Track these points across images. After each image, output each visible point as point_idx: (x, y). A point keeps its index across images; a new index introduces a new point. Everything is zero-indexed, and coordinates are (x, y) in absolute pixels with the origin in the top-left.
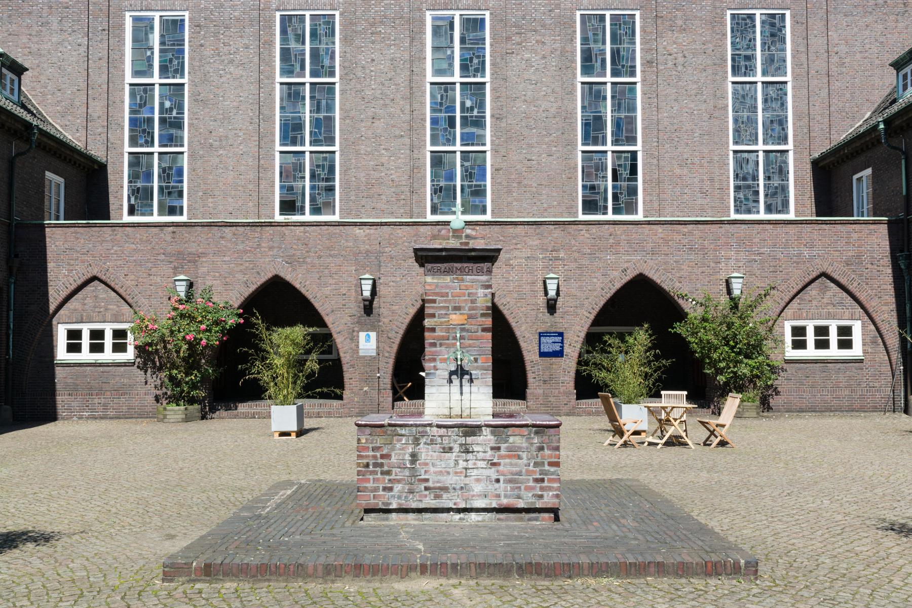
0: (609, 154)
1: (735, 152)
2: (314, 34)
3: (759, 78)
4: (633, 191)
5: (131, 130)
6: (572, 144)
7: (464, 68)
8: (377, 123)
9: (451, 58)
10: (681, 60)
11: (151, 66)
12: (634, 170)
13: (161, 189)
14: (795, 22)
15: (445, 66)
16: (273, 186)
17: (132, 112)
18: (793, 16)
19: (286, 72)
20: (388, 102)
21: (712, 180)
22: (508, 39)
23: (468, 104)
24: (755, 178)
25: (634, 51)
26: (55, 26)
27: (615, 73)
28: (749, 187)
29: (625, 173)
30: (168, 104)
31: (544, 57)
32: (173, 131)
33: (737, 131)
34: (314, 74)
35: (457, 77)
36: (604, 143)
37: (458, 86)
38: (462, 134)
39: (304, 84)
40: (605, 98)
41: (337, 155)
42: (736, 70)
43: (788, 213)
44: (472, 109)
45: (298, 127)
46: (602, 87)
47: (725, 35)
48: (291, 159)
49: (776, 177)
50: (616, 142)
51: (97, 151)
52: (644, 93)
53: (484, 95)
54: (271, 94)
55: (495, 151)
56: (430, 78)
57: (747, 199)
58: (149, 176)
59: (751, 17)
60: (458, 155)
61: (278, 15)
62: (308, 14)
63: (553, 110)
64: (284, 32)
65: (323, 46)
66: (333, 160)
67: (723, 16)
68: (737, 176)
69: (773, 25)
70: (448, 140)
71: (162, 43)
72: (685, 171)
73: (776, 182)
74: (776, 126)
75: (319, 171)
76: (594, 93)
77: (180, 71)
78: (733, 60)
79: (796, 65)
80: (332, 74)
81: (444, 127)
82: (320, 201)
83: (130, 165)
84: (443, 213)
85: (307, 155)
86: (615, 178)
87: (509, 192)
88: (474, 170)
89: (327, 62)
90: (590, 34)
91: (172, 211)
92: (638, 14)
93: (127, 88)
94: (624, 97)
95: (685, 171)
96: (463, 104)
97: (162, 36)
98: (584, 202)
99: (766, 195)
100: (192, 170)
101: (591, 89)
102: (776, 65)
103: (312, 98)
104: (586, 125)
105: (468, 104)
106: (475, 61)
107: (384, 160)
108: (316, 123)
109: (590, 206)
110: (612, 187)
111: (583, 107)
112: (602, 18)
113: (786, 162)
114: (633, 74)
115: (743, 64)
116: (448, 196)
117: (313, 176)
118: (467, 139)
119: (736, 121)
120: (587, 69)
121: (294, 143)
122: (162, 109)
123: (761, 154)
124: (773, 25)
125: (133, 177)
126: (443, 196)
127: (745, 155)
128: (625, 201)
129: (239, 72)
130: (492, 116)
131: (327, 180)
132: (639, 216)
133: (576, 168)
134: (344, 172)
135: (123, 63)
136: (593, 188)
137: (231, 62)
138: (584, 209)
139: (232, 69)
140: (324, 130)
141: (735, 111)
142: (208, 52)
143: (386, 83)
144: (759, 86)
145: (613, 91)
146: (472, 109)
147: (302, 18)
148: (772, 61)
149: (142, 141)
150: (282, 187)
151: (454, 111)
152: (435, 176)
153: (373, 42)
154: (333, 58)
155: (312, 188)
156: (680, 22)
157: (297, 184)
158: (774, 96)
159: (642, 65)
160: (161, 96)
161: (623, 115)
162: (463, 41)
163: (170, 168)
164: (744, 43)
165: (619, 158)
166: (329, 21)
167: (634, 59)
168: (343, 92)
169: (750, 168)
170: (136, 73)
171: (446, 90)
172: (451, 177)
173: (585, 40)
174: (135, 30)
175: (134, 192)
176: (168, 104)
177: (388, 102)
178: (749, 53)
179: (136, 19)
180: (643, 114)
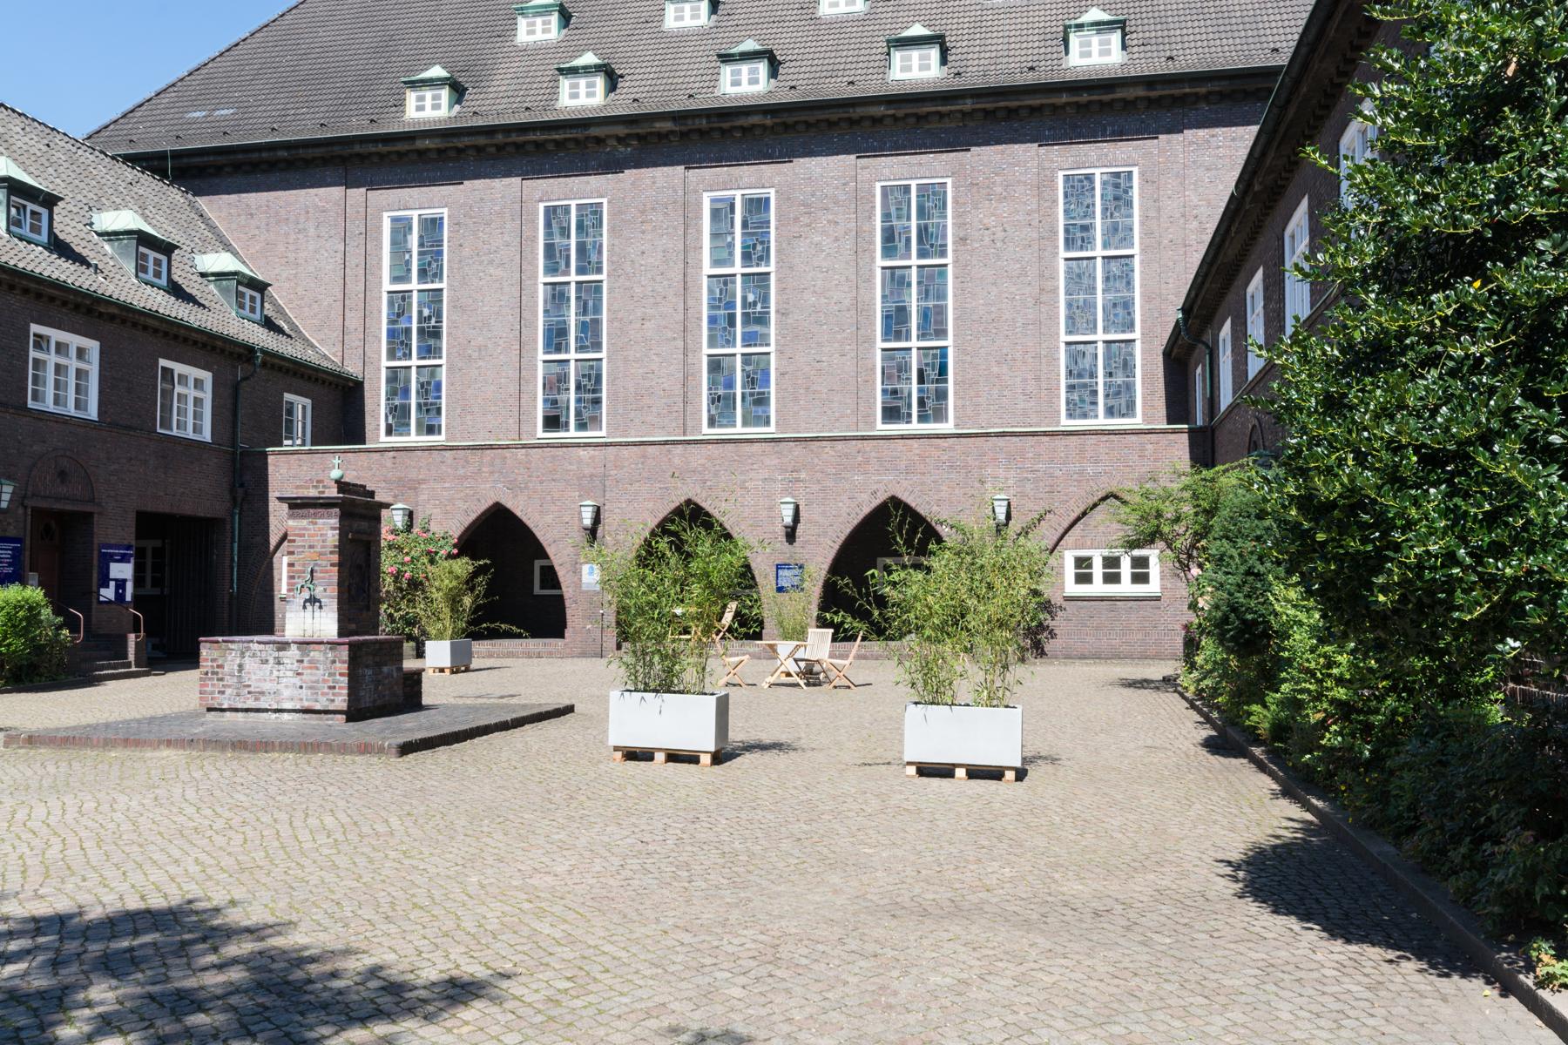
0: (914, 351)
1: (1068, 344)
2: (580, 226)
3: (1099, 251)
4: (942, 395)
5: (389, 343)
6: (870, 341)
7: (747, 257)
8: (647, 324)
9: (731, 245)
10: (1000, 235)
11: (409, 271)
12: (943, 370)
13: (419, 406)
14: (1145, 181)
15: (725, 255)
16: (535, 399)
17: (391, 322)
18: (1142, 174)
19: (552, 269)
20: (659, 299)
21: (1037, 379)
22: (796, 219)
23: (751, 298)
24: (1093, 375)
25: (945, 226)
26: (312, 232)
27: (922, 254)
28: (1085, 386)
29: (932, 374)
30: (426, 312)
31: (837, 240)
32: (431, 342)
33: (1070, 318)
34: (581, 271)
35: (738, 268)
36: (908, 338)
37: (739, 279)
38: (744, 334)
39: (568, 283)
40: (909, 285)
41: (604, 363)
42: (1069, 243)
43: (1134, 416)
44: (755, 303)
45: (563, 332)
46: (906, 272)
47: (1055, 201)
48: (556, 369)
49: (1120, 372)
50: (922, 337)
51: (352, 368)
52: (956, 277)
53: (768, 287)
54: (534, 295)
55: (780, 352)
56: (708, 270)
57: (1082, 401)
58: (406, 391)
59: (1089, 178)
60: (739, 358)
61: (541, 206)
62: (573, 204)
63: (847, 302)
64: (548, 225)
65: (590, 240)
66: (600, 369)
67: (1053, 180)
68: (1070, 373)
69: (1117, 186)
70: (728, 342)
71: (421, 245)
72: (1005, 369)
73: (1119, 379)
74: (1119, 310)
75: (585, 382)
76: (896, 279)
77: (438, 275)
78: (1067, 231)
79: (1146, 234)
80: (599, 270)
81: (722, 326)
82: (586, 415)
83: (388, 381)
84: (721, 426)
85: (572, 363)
86: (921, 380)
87: (796, 400)
88: (757, 377)
89: (594, 258)
90: (893, 209)
91: (431, 430)
92: (949, 181)
93: (385, 297)
94: (932, 282)
95: (1005, 369)
96: (744, 299)
97: (421, 237)
98: (885, 409)
99: (1107, 396)
100: (451, 384)
101: (893, 275)
102: (1121, 235)
103: (578, 298)
104: (887, 318)
105: (751, 298)
106: (759, 248)
107: (654, 367)
108: (583, 327)
109: (891, 414)
110: (918, 390)
111: (884, 297)
112: (907, 189)
113: (1132, 355)
114: (943, 254)
115: (1078, 236)
116: (727, 406)
117: (578, 388)
118: (749, 340)
119: (1069, 305)
120: (889, 251)
121: (558, 350)
122: (421, 319)
123: (1100, 346)
124: (1117, 186)
125: (392, 393)
126: (722, 404)
127: (1081, 347)
128: (932, 407)
129: (499, 272)
130: (777, 311)
131: (594, 391)
132: (947, 427)
133: (873, 369)
134: (611, 382)
135: (380, 268)
136: (895, 392)
137: (491, 262)
138: (884, 417)
139: (492, 271)
140: (590, 335)
141: (1068, 293)
142: (466, 252)
143: (658, 278)
144: (1099, 262)
145: (920, 276)
146: (755, 303)
147: (567, 209)
148: (1116, 230)
149: (399, 354)
150: (545, 401)
151: (734, 307)
152: (713, 384)
153: (643, 232)
154: (600, 252)
155: (578, 401)
156: (999, 189)
157: (561, 397)
158: (1118, 273)
159: (954, 243)
160: (420, 304)
161: (931, 304)
162: (745, 225)
163: (429, 383)
164: (1081, 210)
165: (926, 356)
166: (596, 210)
167: (944, 236)
168: (610, 291)
169: (1086, 363)
170: (396, 279)
171: (725, 283)
172: (730, 384)
173: (886, 216)
174: (394, 231)
175: (392, 410)
176: (426, 312)
177: (659, 299)
178: (1086, 222)
179: (394, 220)
180: (955, 302)
